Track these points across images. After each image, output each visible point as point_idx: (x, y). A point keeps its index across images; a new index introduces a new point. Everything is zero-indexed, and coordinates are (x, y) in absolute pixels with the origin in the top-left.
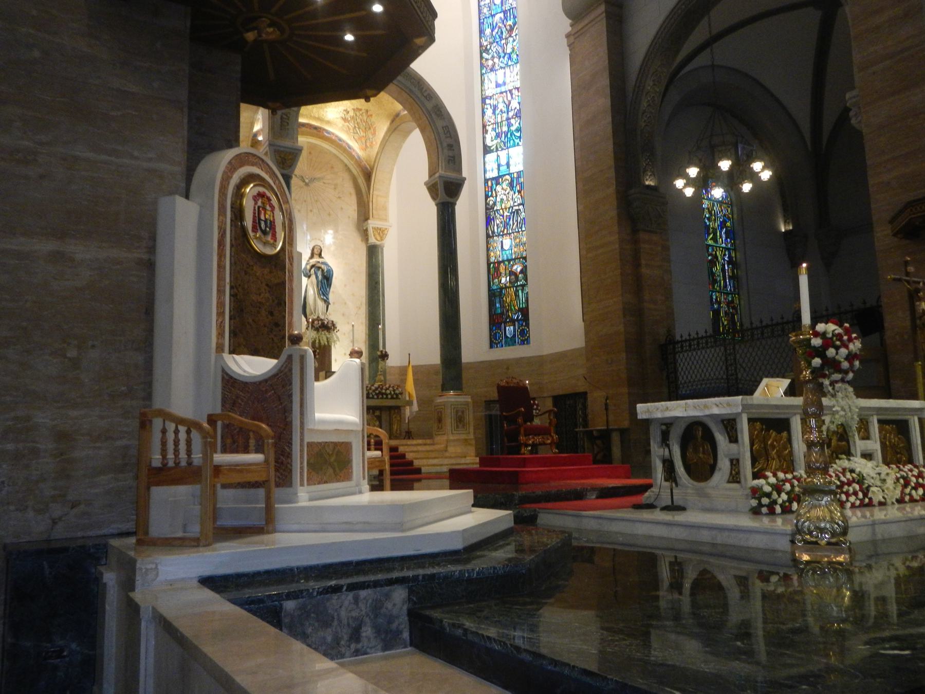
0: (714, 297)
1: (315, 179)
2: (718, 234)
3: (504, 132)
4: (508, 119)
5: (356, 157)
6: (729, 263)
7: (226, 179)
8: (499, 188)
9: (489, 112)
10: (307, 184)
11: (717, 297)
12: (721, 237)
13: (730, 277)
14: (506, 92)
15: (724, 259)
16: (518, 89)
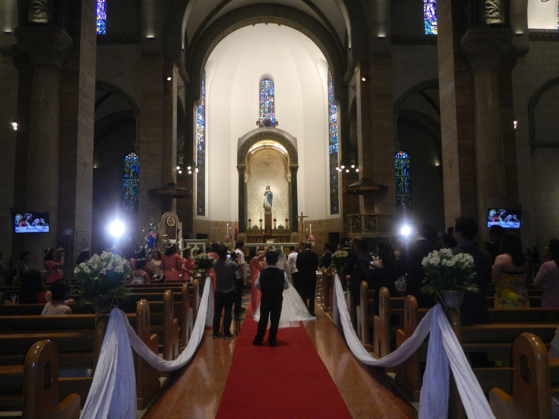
0: (398, 196)
1: (270, 163)
2: (402, 171)
3: (335, 138)
4: (335, 133)
5: (284, 153)
6: (407, 182)
7: (164, 218)
8: (333, 158)
9: (331, 130)
10: (268, 165)
11: (399, 195)
12: (403, 172)
13: (407, 187)
14: (334, 122)
15: (405, 181)
16: (337, 121)
